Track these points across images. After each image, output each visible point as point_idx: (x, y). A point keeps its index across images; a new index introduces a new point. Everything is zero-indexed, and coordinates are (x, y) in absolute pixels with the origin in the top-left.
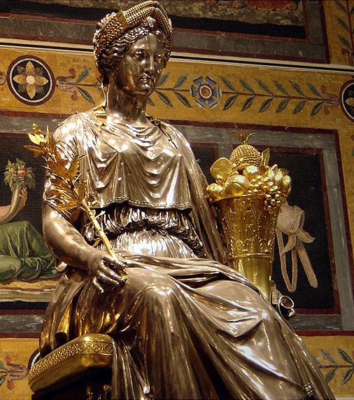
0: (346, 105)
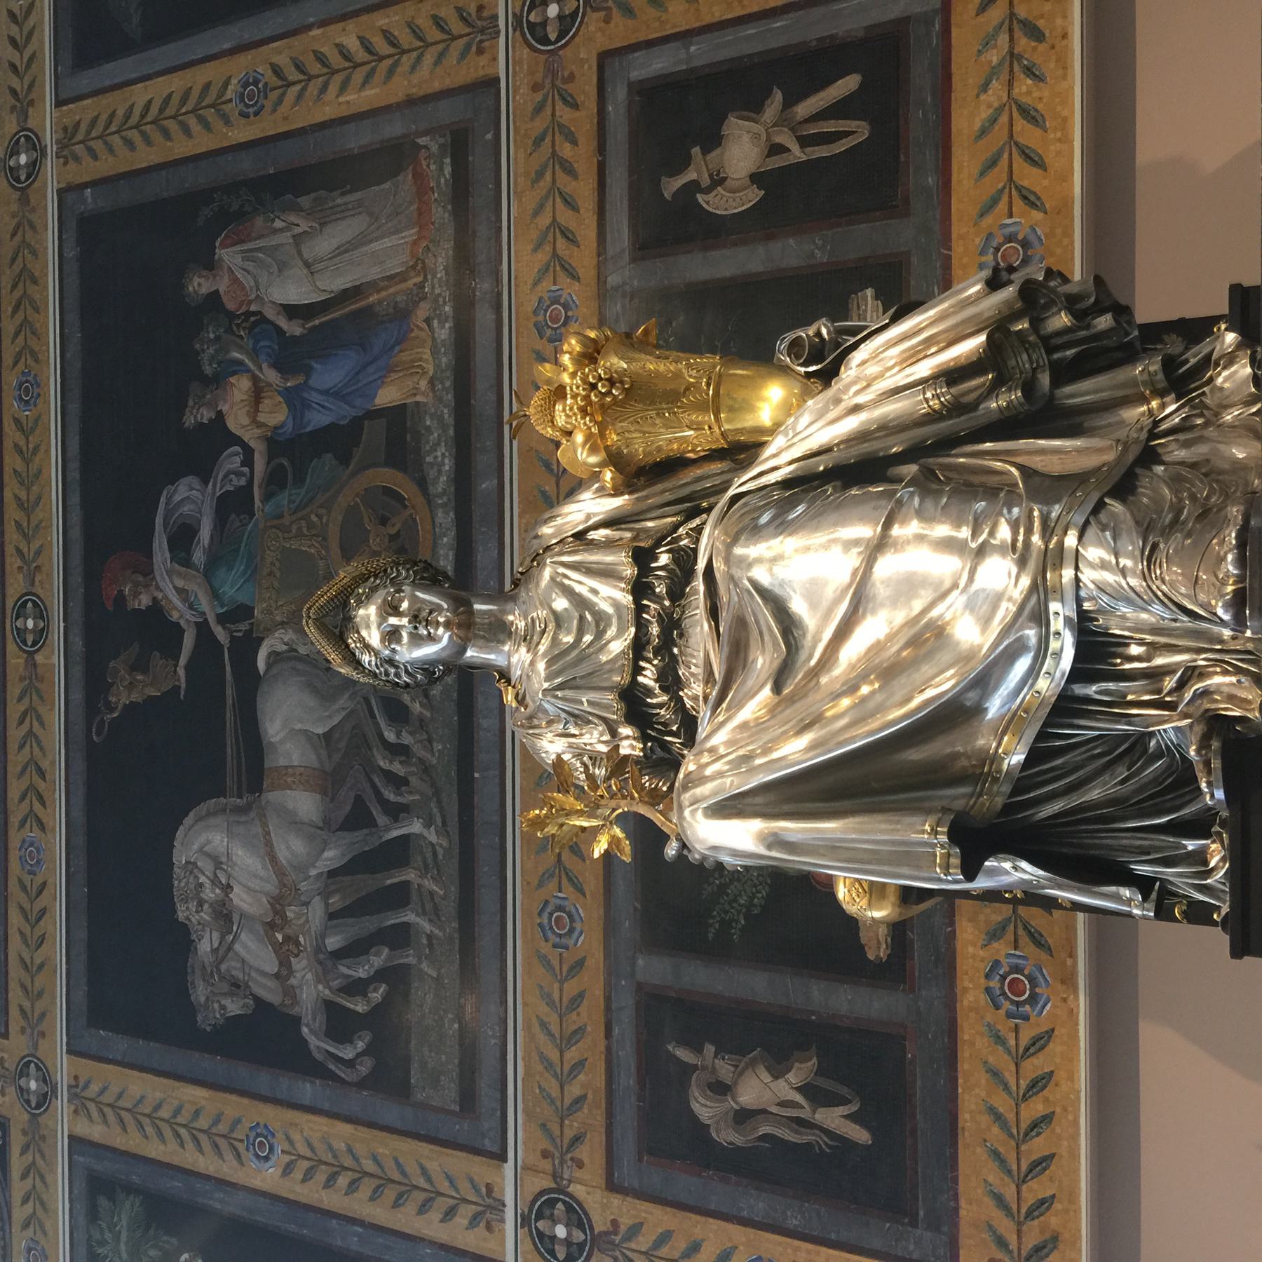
0: (559, 39)
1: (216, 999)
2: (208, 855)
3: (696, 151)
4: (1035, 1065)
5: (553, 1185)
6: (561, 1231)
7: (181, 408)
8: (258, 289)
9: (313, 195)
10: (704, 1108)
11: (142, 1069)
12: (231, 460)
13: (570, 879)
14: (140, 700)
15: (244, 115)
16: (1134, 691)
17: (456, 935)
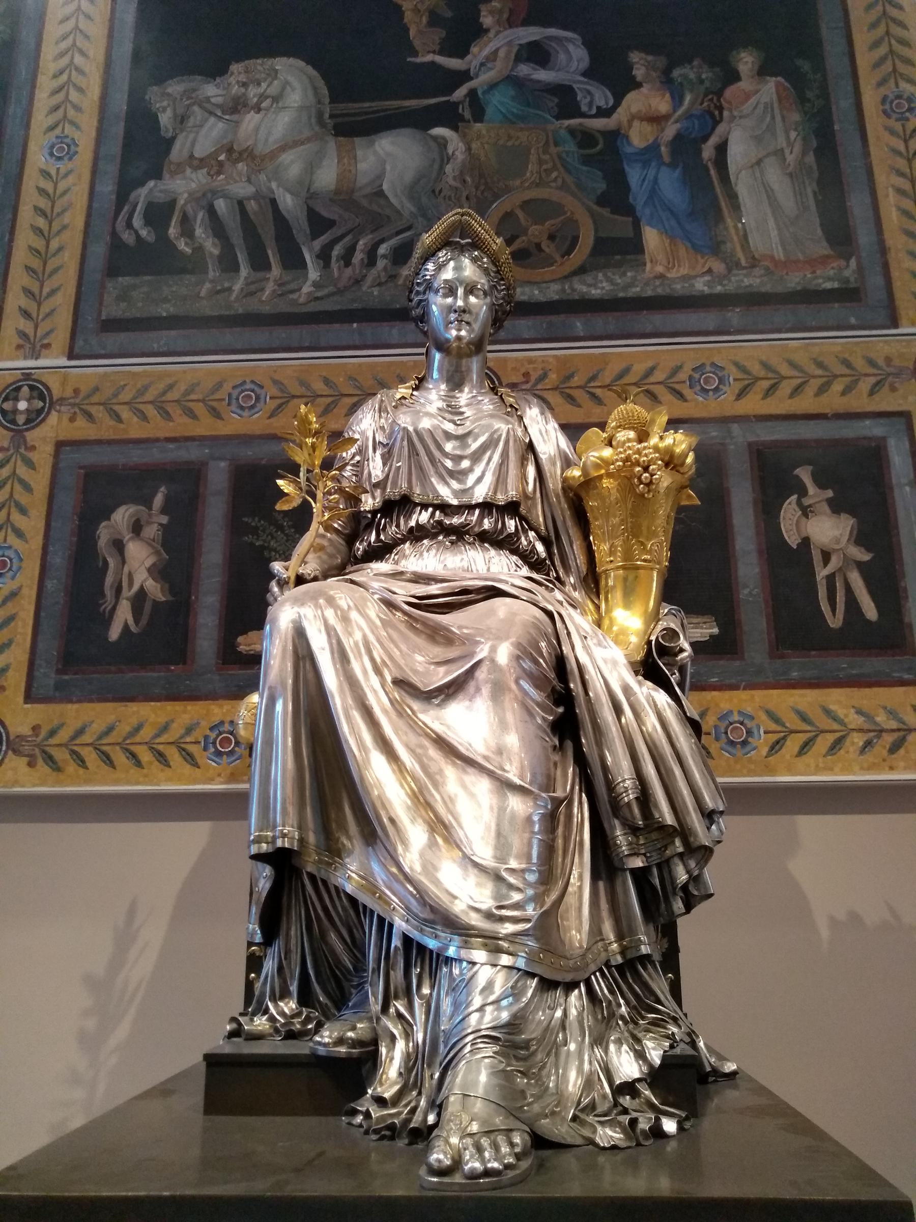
1: (171, 103)
2: (283, 89)
3: (830, 493)
4: (173, 754)
5: (55, 398)
6: (22, 405)
7: (646, 49)
8: (741, 117)
9: (815, 167)
10: (122, 516)
11: (110, 36)
12: (602, 97)
13: (280, 406)
14: (406, 20)
15: (884, 99)
16: (397, 975)
17: (232, 312)
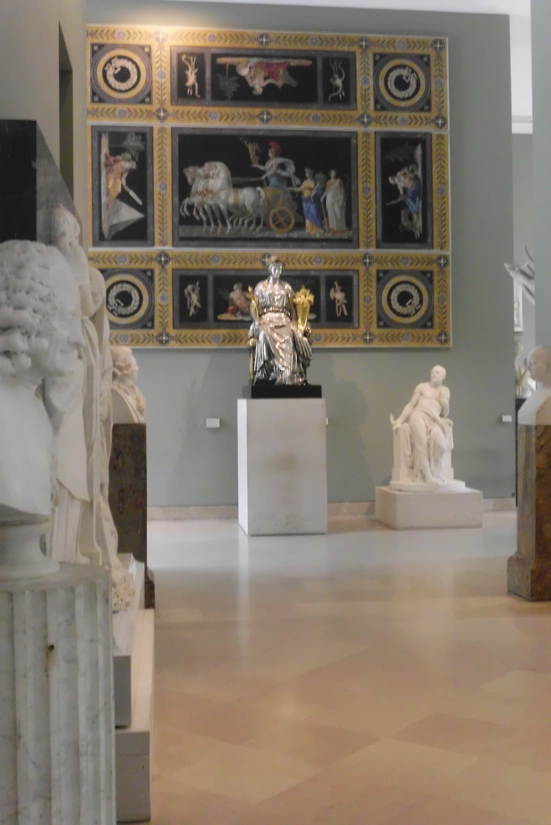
10: (190, 287)
12: (298, 181)
